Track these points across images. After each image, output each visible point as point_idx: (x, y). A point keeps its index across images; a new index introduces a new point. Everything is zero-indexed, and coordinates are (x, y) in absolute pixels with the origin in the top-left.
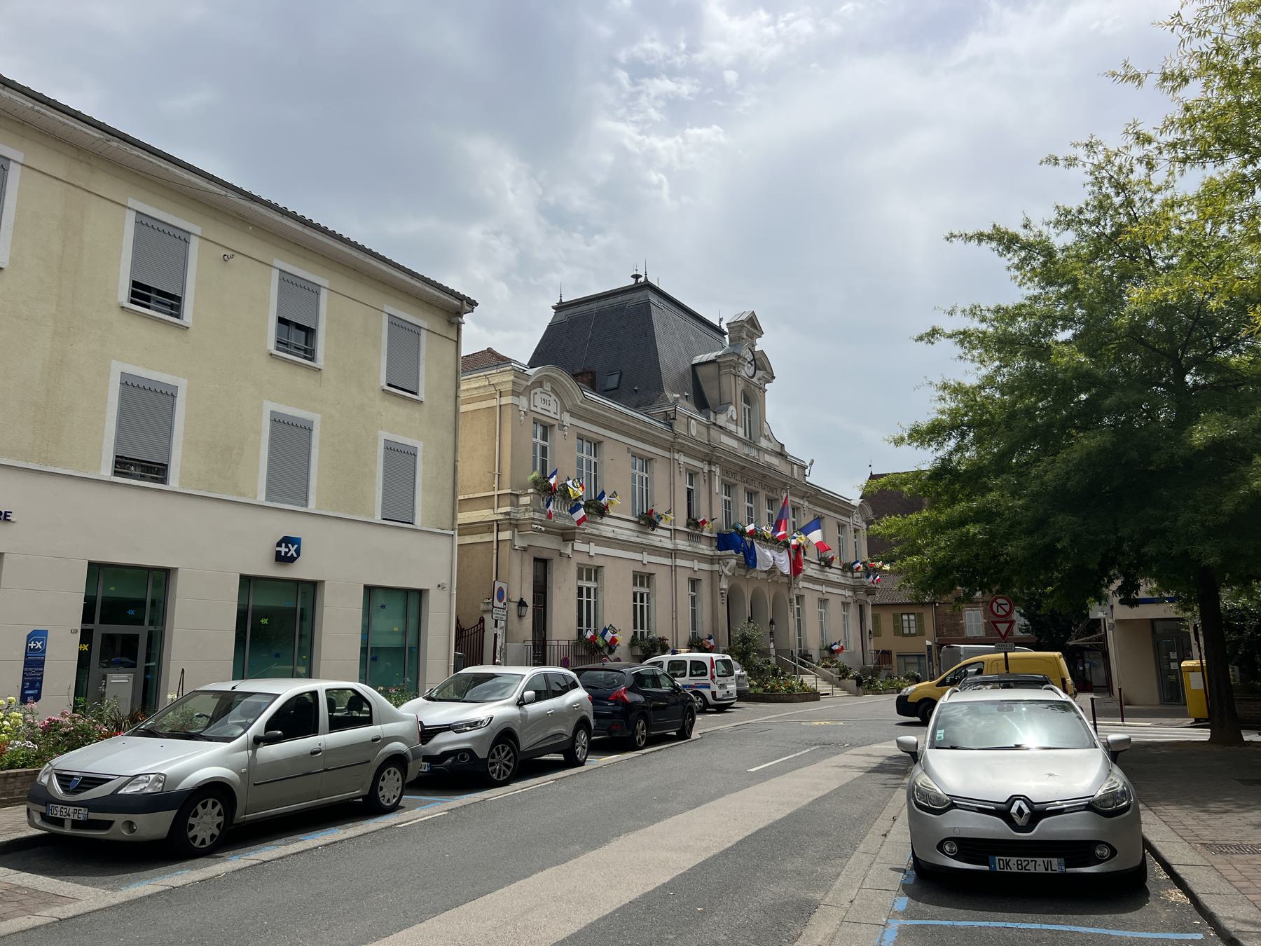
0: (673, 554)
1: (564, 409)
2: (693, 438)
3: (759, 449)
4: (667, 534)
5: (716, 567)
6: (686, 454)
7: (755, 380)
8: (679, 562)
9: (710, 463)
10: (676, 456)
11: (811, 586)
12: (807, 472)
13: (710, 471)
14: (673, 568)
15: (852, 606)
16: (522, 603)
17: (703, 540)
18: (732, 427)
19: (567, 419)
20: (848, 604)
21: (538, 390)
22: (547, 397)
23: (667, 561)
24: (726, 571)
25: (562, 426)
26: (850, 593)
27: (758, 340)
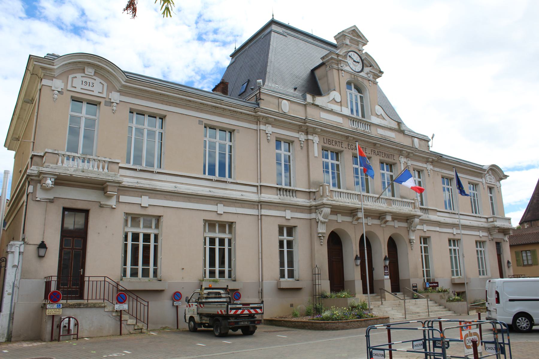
0: (260, 204)
1: (111, 88)
2: (284, 114)
3: (370, 124)
4: (254, 189)
5: (313, 216)
6: (273, 126)
7: (361, 74)
8: (264, 212)
9: (307, 133)
10: (262, 127)
11: (438, 229)
12: (430, 143)
13: (307, 140)
14: (260, 217)
15: (488, 244)
16: (43, 246)
17: (298, 194)
18: (336, 108)
19: (115, 97)
20: (484, 242)
21: (79, 75)
22: (88, 80)
23: (254, 212)
24: (321, 219)
25: (110, 103)
26: (485, 234)
27: (364, 47)
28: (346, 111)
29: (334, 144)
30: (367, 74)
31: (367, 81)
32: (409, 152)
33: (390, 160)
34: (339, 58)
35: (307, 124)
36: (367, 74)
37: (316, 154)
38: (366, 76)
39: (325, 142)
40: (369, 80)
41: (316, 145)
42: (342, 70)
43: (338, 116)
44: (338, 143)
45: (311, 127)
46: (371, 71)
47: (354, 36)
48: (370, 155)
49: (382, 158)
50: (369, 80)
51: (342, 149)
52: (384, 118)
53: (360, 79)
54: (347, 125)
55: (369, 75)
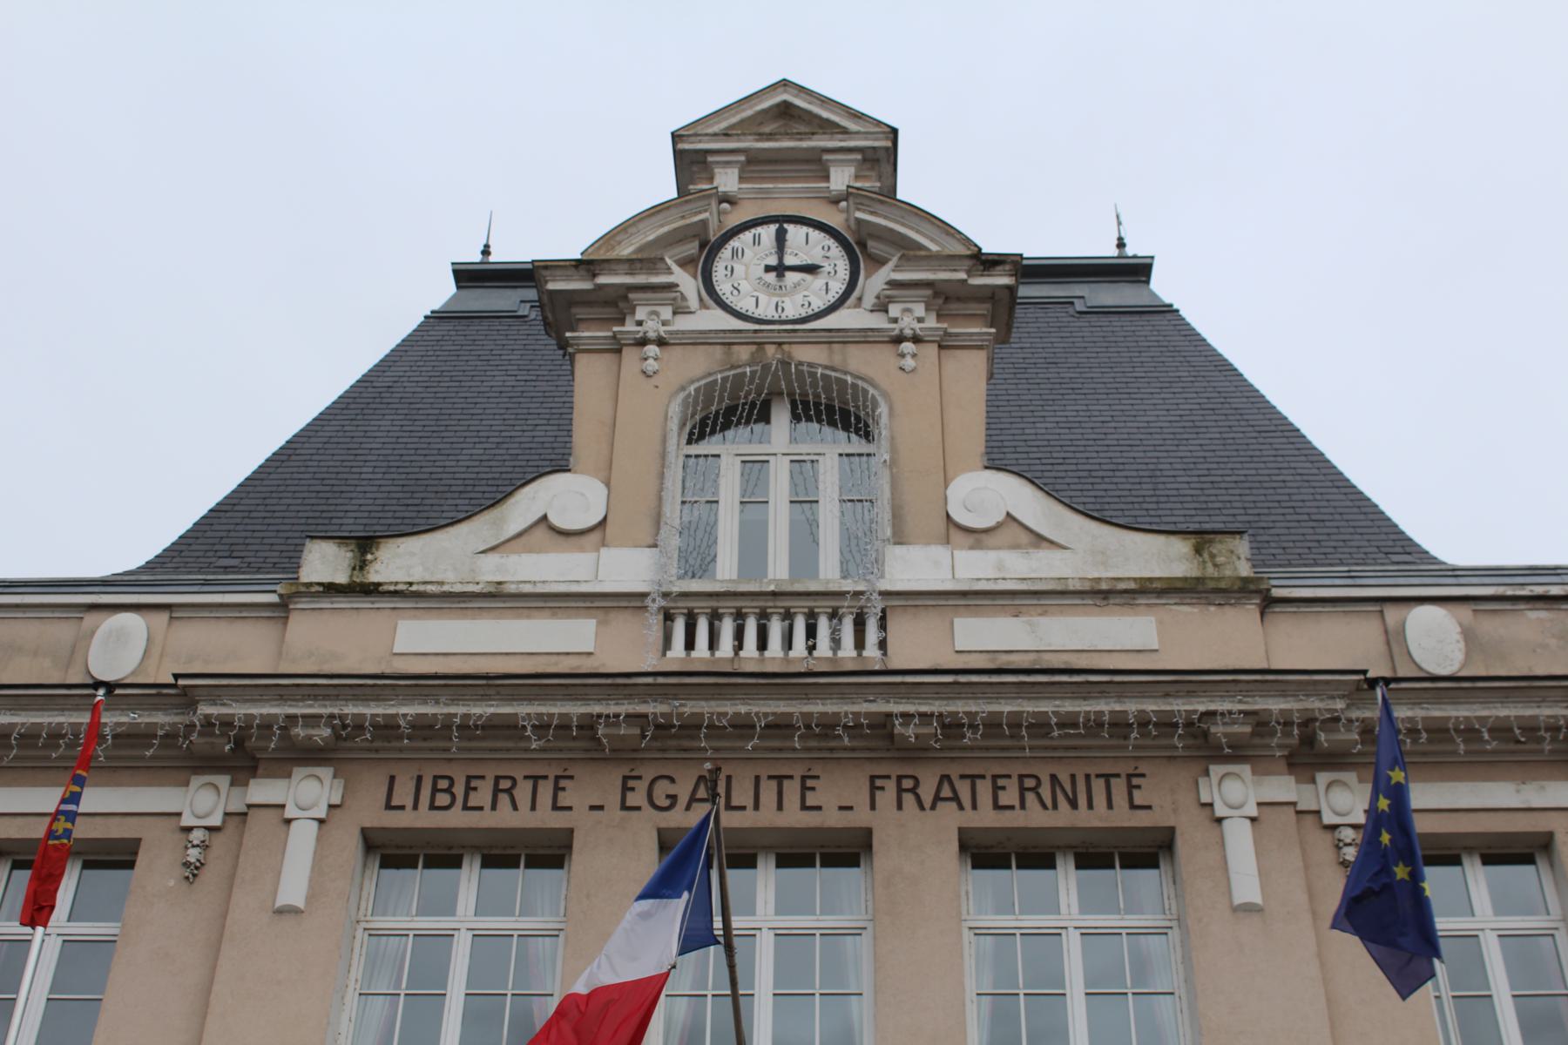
28: (626, 568)
29: (483, 796)
30: (881, 307)
31: (885, 354)
32: (1308, 722)
33: (1102, 815)
34: (602, 280)
35: (205, 709)
36: (881, 307)
37: (293, 890)
38: (877, 321)
39: (403, 795)
40: (898, 340)
41: (303, 837)
42: (643, 342)
43: (555, 612)
44: (523, 792)
45: (266, 725)
46: (893, 284)
47: (770, 136)
48: (861, 817)
49: (985, 818)
50: (898, 340)
51: (557, 821)
52: (1039, 540)
53: (805, 354)
54: (632, 648)
55: (894, 310)
